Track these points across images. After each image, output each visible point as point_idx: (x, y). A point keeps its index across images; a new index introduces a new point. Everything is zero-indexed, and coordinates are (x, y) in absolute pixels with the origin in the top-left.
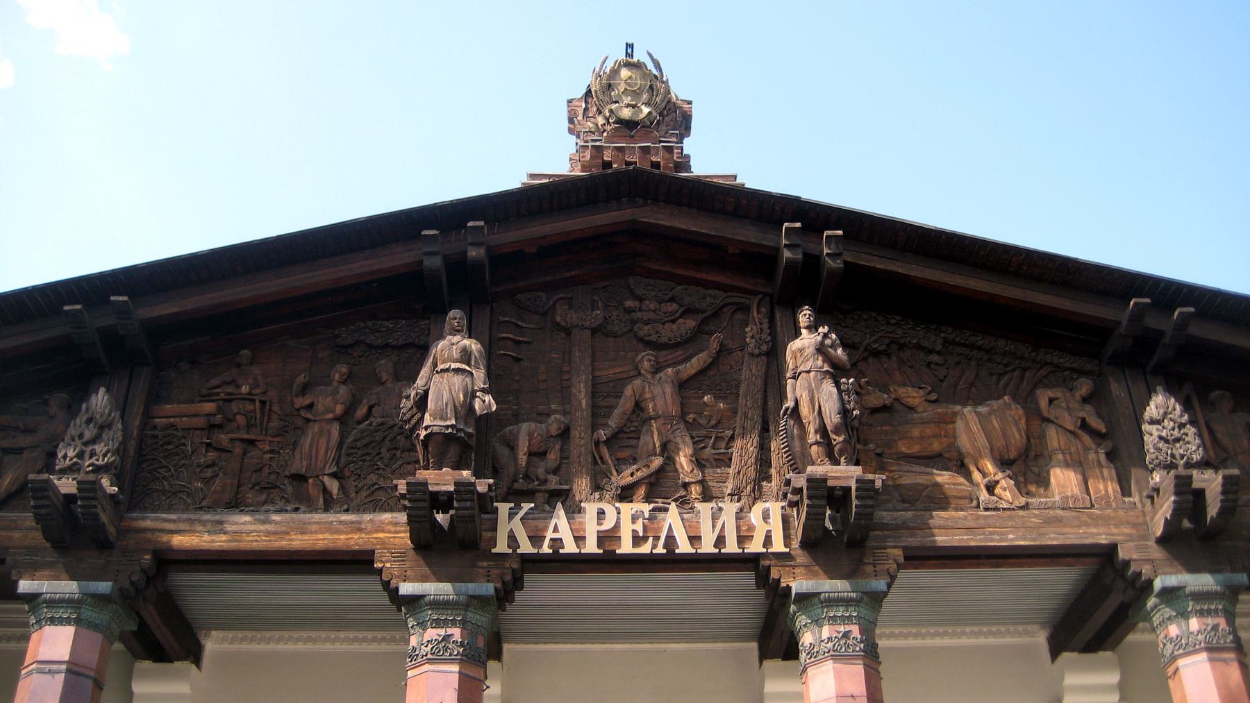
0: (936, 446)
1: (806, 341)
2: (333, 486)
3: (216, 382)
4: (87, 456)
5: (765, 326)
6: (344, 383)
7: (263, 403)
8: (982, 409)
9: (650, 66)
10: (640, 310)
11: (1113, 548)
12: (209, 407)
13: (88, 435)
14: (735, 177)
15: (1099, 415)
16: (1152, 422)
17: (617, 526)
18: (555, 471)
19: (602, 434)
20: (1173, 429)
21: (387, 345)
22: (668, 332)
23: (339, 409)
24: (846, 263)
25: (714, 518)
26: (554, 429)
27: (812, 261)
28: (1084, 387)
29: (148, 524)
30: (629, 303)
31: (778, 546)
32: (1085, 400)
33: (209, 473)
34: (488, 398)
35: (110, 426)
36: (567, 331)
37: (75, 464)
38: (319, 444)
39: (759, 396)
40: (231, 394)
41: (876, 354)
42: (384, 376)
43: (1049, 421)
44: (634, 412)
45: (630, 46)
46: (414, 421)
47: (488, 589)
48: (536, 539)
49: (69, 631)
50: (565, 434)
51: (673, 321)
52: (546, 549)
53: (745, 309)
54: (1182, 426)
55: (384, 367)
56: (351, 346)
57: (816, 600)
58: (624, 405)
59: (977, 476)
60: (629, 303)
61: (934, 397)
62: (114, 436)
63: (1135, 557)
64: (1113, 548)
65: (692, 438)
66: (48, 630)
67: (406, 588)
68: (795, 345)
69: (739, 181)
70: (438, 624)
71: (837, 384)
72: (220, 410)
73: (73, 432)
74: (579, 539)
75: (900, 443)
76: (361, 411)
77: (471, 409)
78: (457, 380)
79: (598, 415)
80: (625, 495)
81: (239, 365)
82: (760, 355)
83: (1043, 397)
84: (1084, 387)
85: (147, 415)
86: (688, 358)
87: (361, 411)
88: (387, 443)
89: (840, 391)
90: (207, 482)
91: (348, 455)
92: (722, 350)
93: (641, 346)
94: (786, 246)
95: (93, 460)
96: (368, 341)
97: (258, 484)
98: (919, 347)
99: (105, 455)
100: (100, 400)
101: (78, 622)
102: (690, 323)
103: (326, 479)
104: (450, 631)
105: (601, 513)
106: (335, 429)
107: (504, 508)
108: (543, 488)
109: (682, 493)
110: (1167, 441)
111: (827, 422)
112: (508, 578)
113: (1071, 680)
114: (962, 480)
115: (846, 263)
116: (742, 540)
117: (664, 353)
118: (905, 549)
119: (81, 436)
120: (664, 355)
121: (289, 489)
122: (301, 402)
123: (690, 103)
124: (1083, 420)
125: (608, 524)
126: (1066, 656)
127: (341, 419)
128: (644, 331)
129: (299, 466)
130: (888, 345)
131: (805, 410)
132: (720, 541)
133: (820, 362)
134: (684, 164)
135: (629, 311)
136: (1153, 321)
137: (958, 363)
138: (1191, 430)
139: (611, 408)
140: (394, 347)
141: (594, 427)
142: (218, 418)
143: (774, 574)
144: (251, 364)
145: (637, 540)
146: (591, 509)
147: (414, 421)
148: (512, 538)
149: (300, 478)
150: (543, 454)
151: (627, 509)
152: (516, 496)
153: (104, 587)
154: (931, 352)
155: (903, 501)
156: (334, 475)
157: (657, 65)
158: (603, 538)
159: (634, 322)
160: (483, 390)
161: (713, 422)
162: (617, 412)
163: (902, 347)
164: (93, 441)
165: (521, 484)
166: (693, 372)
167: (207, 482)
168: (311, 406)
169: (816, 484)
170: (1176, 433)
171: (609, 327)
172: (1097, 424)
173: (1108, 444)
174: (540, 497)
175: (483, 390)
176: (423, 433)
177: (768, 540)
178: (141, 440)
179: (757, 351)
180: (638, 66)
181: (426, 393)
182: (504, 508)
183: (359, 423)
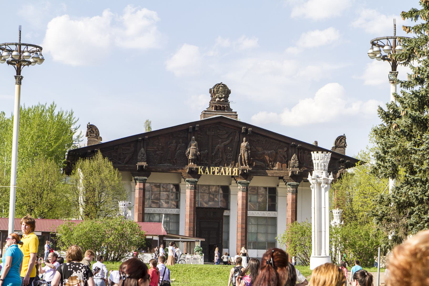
12: (156, 147)
18: (206, 160)
25: (228, 170)
31: (237, 175)
50: (208, 154)
77: (196, 154)
80: (216, 165)
86: (227, 141)
92: (232, 139)
100: (142, 149)
107: (200, 167)
116: (232, 173)
122: (169, 147)
131: (243, 157)
132: (229, 174)
145: (218, 173)
146: (211, 168)
148: (201, 173)
151: (216, 168)
177: (235, 174)
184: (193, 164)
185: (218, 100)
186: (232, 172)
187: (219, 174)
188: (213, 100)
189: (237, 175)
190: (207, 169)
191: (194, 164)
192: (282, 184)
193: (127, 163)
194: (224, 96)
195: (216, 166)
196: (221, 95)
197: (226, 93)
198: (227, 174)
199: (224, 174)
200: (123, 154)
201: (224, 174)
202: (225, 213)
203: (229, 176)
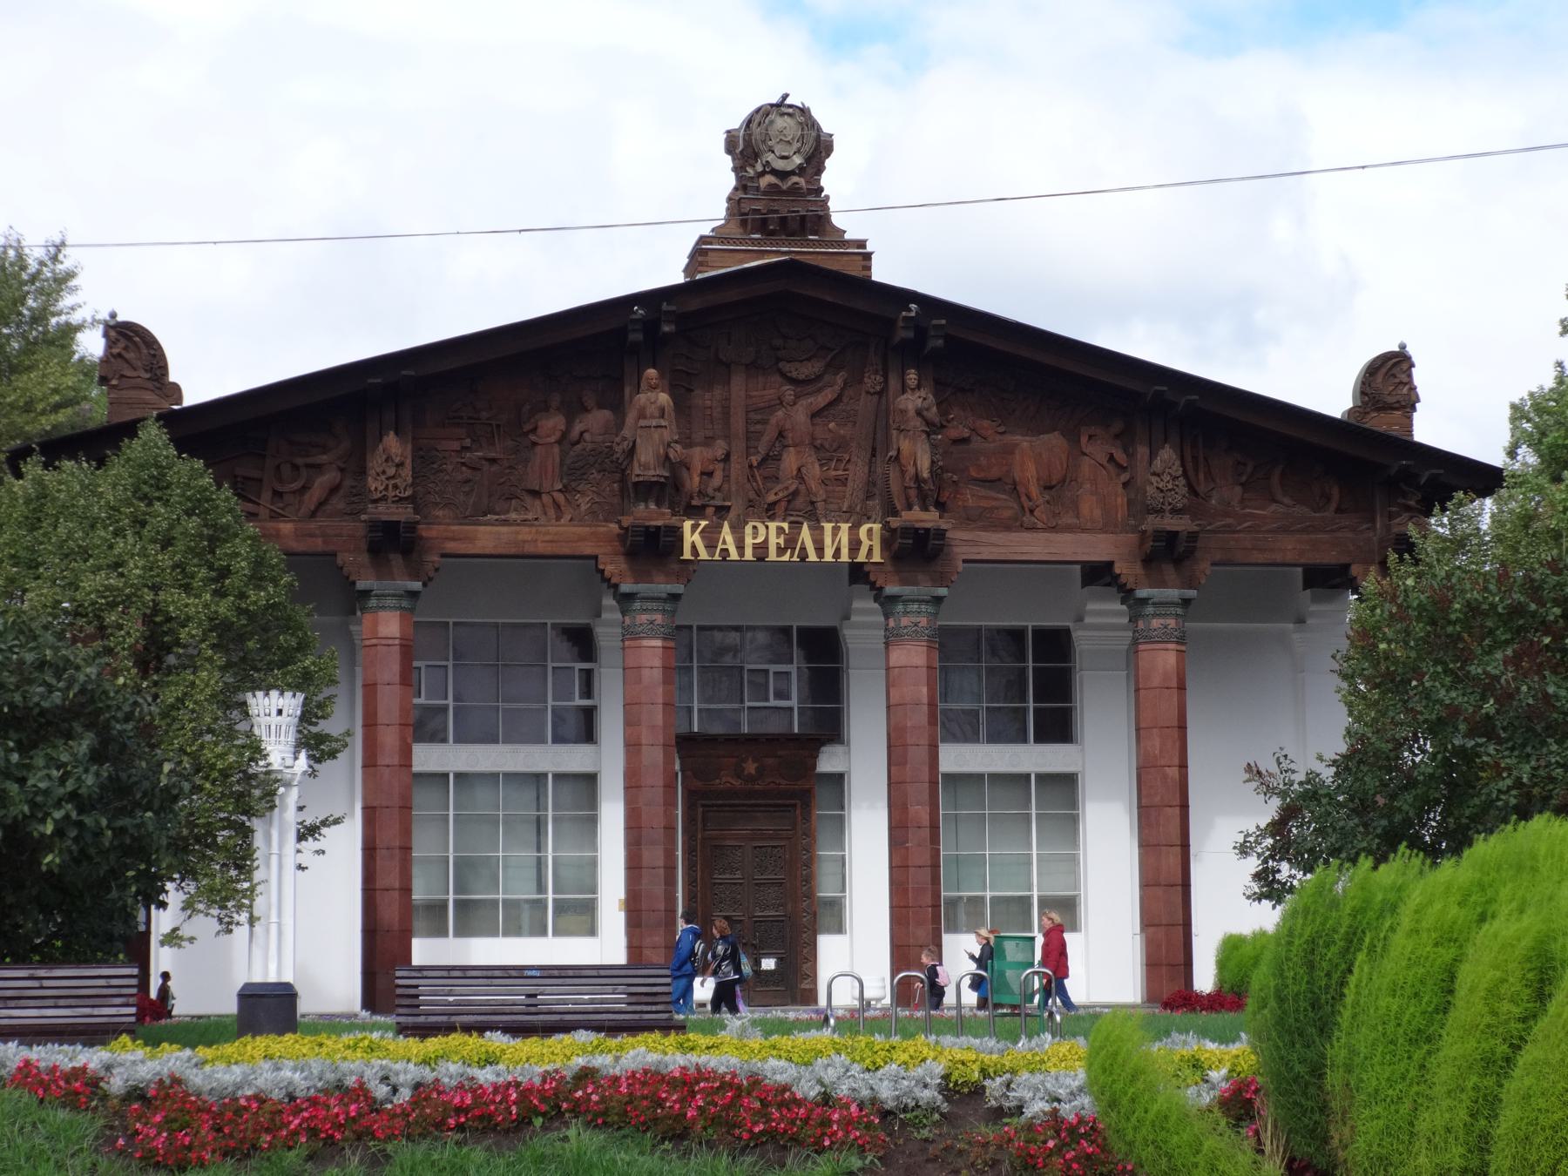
0: (995, 473)
2: (560, 498)
11: (1110, 564)
13: (391, 471)
17: (766, 540)
19: (755, 460)
23: (558, 435)
26: (720, 453)
28: (1117, 426)
29: (434, 533)
31: (877, 558)
32: (1117, 436)
34: (678, 447)
38: (544, 464)
45: (785, 96)
48: (711, 547)
50: (727, 457)
52: (717, 557)
58: (770, 434)
59: (1024, 498)
60: (778, 342)
61: (1002, 429)
64: (1110, 564)
66: (382, 614)
69: (869, 249)
74: (741, 548)
77: (667, 457)
80: (770, 512)
84: (1117, 426)
86: (820, 390)
90: (467, 494)
100: (391, 442)
103: (555, 494)
105: (755, 527)
106: (556, 449)
107: (688, 525)
113: (1091, 606)
119: (384, 472)
121: (528, 499)
122: (527, 427)
125: (760, 540)
127: (559, 442)
139: (761, 433)
142: (468, 442)
145: (781, 551)
148: (694, 547)
150: (710, 474)
151: (773, 525)
152: (695, 512)
158: (756, 547)
161: (835, 445)
162: (766, 438)
164: (393, 477)
167: (467, 494)
172: (1120, 456)
173: (1125, 477)
174: (710, 511)
182: (688, 525)
184: (653, 506)
185: (770, 185)
186: (855, 546)
187: (786, 558)
188: (743, 185)
189: (877, 558)
190: (727, 534)
191: (658, 505)
192: (1105, 610)
194: (798, 160)
195: (772, 518)
197: (807, 148)
198: (828, 557)
199: (813, 557)
200: (296, 467)
201: (813, 557)
202: (828, 762)
203: (835, 566)
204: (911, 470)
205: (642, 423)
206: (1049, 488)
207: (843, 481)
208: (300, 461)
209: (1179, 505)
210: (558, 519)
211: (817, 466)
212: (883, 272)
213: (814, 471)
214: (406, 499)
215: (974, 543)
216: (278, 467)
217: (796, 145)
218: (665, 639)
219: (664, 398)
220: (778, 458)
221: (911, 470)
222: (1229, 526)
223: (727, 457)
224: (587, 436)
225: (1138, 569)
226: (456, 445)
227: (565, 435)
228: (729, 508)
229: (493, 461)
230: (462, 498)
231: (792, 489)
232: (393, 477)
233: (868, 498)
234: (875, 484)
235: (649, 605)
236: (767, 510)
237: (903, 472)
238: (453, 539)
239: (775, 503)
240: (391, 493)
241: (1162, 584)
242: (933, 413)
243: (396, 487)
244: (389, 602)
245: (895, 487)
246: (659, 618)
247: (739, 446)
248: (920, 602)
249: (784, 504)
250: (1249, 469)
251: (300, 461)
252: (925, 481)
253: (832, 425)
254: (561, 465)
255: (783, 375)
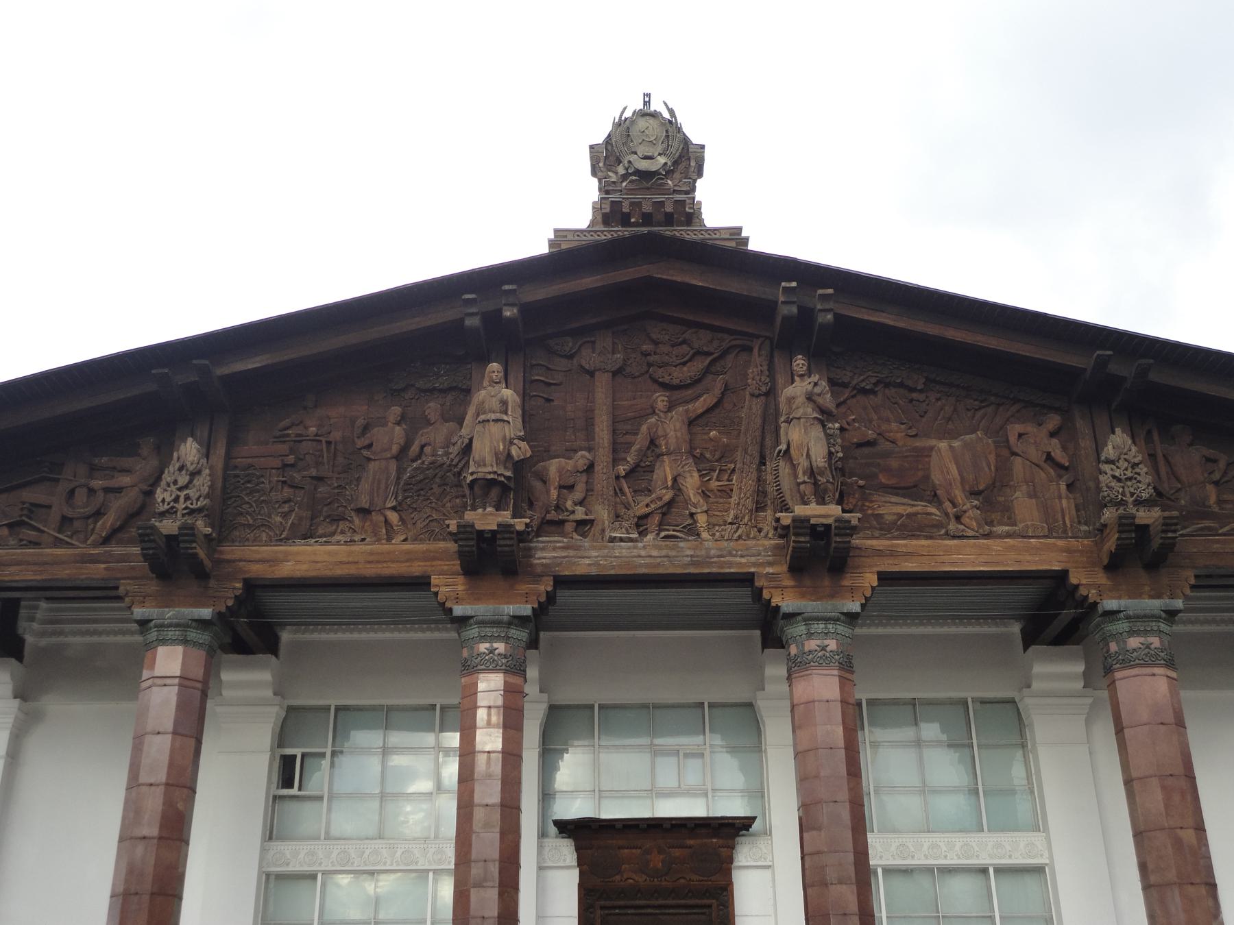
1: (798, 389)
3: (286, 422)
4: (182, 499)
5: (765, 368)
6: (398, 423)
7: (329, 443)
8: (956, 444)
9: (666, 115)
10: (655, 353)
11: (1064, 574)
12: (283, 448)
13: (183, 479)
14: (740, 229)
15: (1064, 448)
16: (1108, 462)
18: (581, 503)
19: (622, 469)
20: (1126, 469)
21: (434, 389)
22: (678, 375)
23: (395, 449)
24: (837, 316)
27: (806, 314)
30: (645, 347)
33: (286, 508)
34: (523, 445)
35: (199, 472)
36: (591, 374)
37: (173, 507)
39: (758, 433)
40: (300, 435)
41: (864, 392)
42: (432, 418)
43: (1017, 454)
44: (648, 448)
46: (460, 465)
47: (526, 610)
49: (179, 650)
50: (590, 468)
51: (684, 364)
53: (749, 349)
54: (1135, 465)
55: (433, 408)
56: (404, 390)
57: (799, 618)
58: (640, 442)
62: (203, 483)
63: (1084, 582)
64: (1064, 574)
65: (699, 471)
66: (161, 650)
67: (458, 610)
68: (789, 391)
69: (744, 234)
70: (483, 638)
71: (824, 426)
72: (292, 451)
73: (169, 479)
75: (881, 476)
76: (415, 448)
77: (509, 455)
78: (495, 429)
79: (618, 451)
81: (305, 408)
82: (760, 395)
83: (1014, 429)
84: (1053, 421)
85: (228, 456)
86: (697, 398)
87: (415, 448)
88: (437, 480)
89: (828, 436)
90: (285, 515)
91: (405, 491)
93: (656, 386)
94: (783, 302)
95: (188, 503)
96: (418, 385)
97: (328, 516)
98: (901, 385)
99: (198, 500)
100: (189, 450)
101: (185, 642)
102: (700, 364)
104: (495, 645)
106: (393, 466)
108: (572, 517)
109: (689, 521)
110: (1119, 480)
111: (814, 464)
112: (543, 599)
113: (1038, 669)
114: (934, 510)
115: (836, 316)
117: (677, 392)
118: (879, 573)
119: (175, 482)
120: (678, 394)
121: (357, 521)
122: (360, 443)
123: (703, 147)
124: (1049, 454)
126: (1033, 648)
128: (660, 373)
129: (364, 502)
130: (876, 384)
133: (810, 410)
134: (691, 215)
135: (646, 354)
136: (1114, 368)
137: (938, 400)
138: (1143, 469)
139: (629, 445)
140: (441, 391)
141: (615, 462)
142: (291, 459)
143: (766, 595)
144: (316, 406)
147: (460, 465)
149: (364, 512)
150: (571, 488)
153: (206, 613)
154: (912, 390)
155: (881, 529)
156: (394, 508)
157: (672, 112)
159: (650, 365)
160: (520, 438)
163: (887, 385)
164: (186, 487)
165: (552, 515)
166: (701, 411)
167: (285, 515)
168: (370, 446)
169: (801, 524)
170: (1129, 474)
171: (628, 370)
172: (1059, 455)
173: (1067, 478)
174: (569, 527)
175: (520, 438)
176: (470, 478)
178: (225, 479)
179: (757, 392)
180: (655, 115)
181: (471, 440)
183: (413, 461)
193: (106, 541)
194: (662, 160)
196: (648, 169)
200: (92, 491)
204: (803, 463)
205: (482, 417)
206: (975, 493)
207: (726, 492)
208: (97, 483)
209: (1145, 496)
210: (389, 539)
211: (696, 474)
212: (752, 246)
213: (691, 482)
214: (200, 510)
215: (892, 554)
216: (72, 493)
217: (660, 148)
218: (506, 672)
219: (508, 393)
220: (650, 470)
221: (803, 463)
222: (1209, 528)
223: (590, 468)
224: (428, 450)
225: (1102, 579)
226: (277, 463)
227: (404, 449)
228: (591, 522)
229: (320, 479)
230: (279, 519)
231: (667, 498)
232: (186, 487)
233: (757, 510)
234: (765, 493)
235: (488, 631)
236: (638, 525)
237: (794, 467)
238: (257, 561)
239: (646, 516)
240: (181, 505)
241: (1135, 594)
242: (828, 400)
243: (187, 498)
244: (172, 634)
245: (786, 484)
246: (500, 647)
247: (603, 457)
248: (827, 620)
249: (657, 518)
250: (1222, 464)
251: (97, 483)
252: (822, 473)
253: (713, 433)
254: (398, 478)
255: (655, 381)
